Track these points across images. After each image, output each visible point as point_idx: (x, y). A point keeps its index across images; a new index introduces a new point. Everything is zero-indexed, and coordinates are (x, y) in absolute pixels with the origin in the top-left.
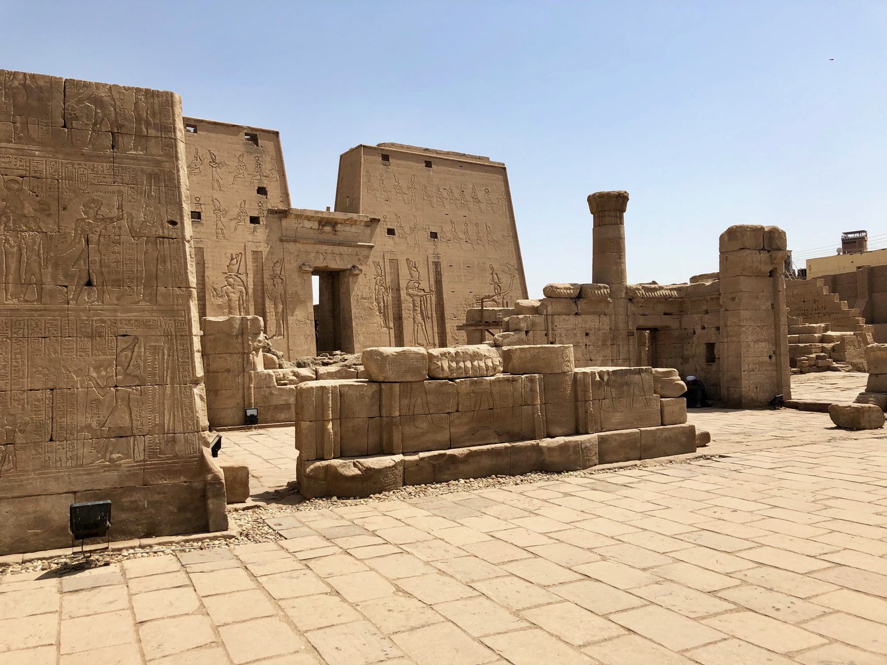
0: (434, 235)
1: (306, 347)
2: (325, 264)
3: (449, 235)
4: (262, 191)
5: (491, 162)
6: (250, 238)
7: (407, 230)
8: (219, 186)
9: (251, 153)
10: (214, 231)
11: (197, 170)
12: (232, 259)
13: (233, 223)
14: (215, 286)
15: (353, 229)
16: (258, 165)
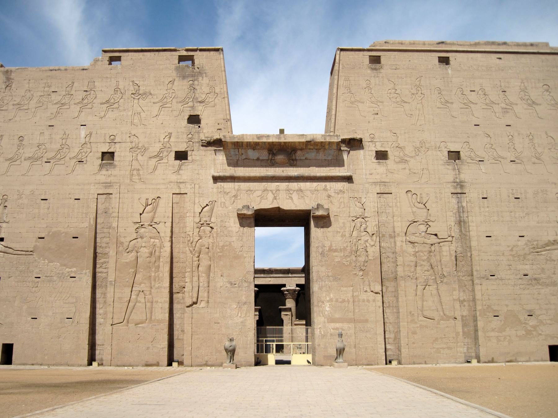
0: (455, 155)
1: (238, 320)
2: (275, 205)
3: (481, 153)
4: (194, 120)
5: (552, 48)
6: (174, 178)
7: (409, 150)
8: (140, 120)
9: (184, 77)
10: (128, 173)
11: (116, 105)
12: (147, 205)
13: (153, 162)
14: (122, 239)
15: (321, 156)
16: (193, 88)
